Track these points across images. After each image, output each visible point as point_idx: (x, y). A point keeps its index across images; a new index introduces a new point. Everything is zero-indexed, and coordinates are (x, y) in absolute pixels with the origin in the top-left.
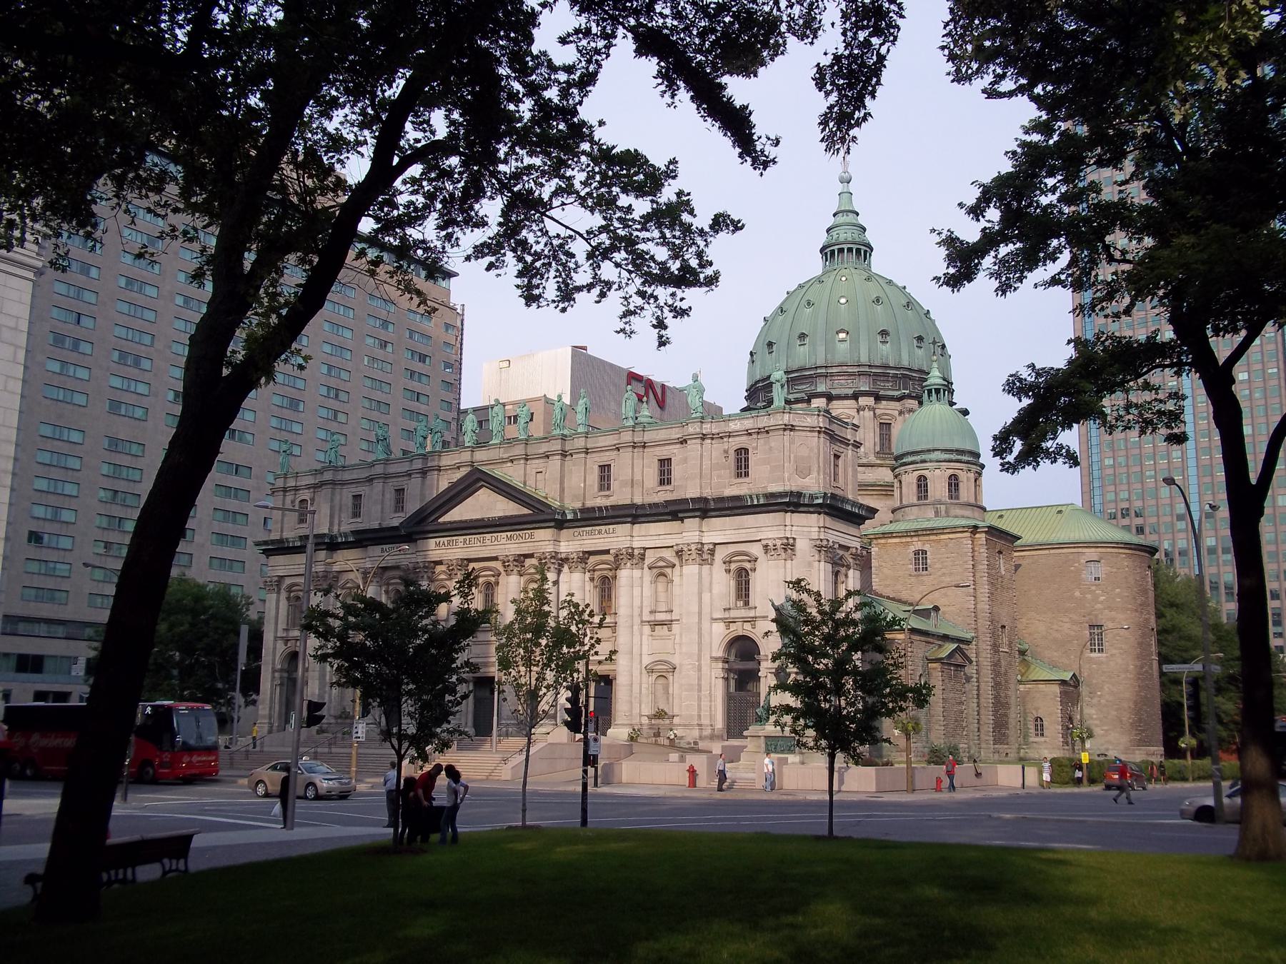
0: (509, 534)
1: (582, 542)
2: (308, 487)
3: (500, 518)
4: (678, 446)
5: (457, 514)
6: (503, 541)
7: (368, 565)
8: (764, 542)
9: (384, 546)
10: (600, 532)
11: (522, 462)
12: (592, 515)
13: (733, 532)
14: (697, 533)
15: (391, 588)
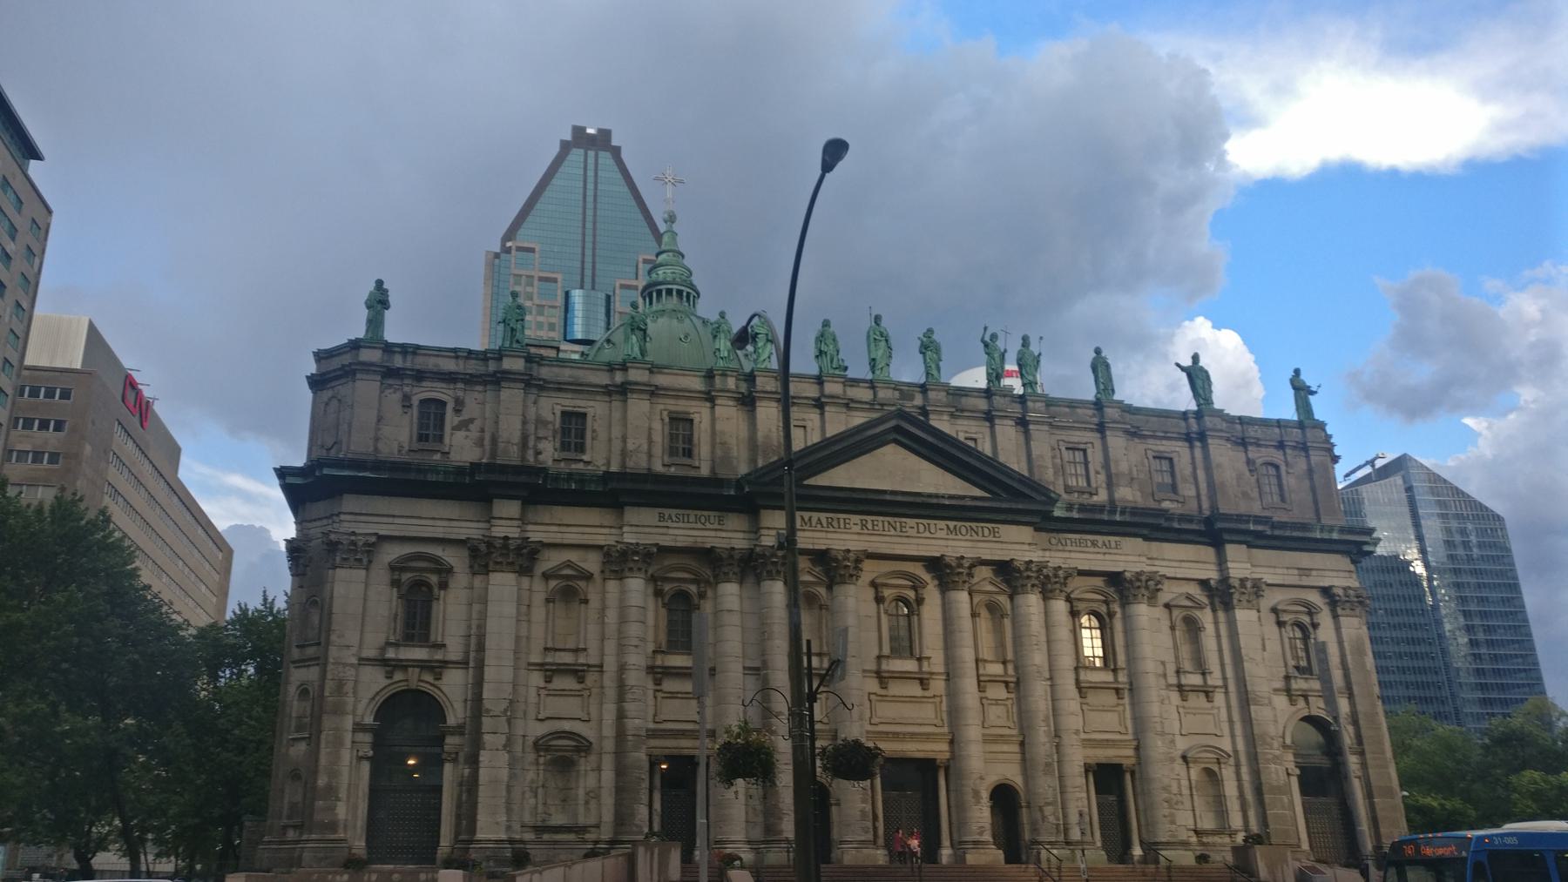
0: (952, 524)
1: (1066, 555)
2: (449, 378)
3: (951, 497)
4: (1180, 443)
5: (840, 477)
6: (943, 534)
7: (629, 538)
8: (1335, 591)
9: (667, 512)
10: (1094, 544)
11: (946, 417)
12: (1098, 516)
13: (1285, 571)
14: (1249, 566)
15: (667, 587)
